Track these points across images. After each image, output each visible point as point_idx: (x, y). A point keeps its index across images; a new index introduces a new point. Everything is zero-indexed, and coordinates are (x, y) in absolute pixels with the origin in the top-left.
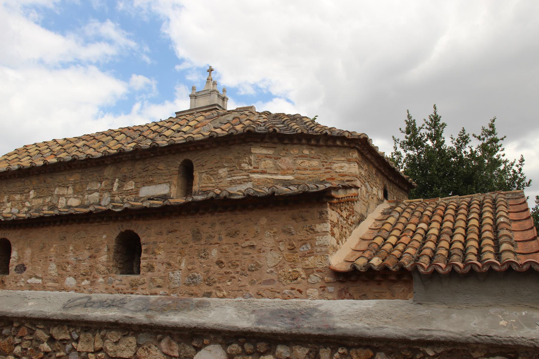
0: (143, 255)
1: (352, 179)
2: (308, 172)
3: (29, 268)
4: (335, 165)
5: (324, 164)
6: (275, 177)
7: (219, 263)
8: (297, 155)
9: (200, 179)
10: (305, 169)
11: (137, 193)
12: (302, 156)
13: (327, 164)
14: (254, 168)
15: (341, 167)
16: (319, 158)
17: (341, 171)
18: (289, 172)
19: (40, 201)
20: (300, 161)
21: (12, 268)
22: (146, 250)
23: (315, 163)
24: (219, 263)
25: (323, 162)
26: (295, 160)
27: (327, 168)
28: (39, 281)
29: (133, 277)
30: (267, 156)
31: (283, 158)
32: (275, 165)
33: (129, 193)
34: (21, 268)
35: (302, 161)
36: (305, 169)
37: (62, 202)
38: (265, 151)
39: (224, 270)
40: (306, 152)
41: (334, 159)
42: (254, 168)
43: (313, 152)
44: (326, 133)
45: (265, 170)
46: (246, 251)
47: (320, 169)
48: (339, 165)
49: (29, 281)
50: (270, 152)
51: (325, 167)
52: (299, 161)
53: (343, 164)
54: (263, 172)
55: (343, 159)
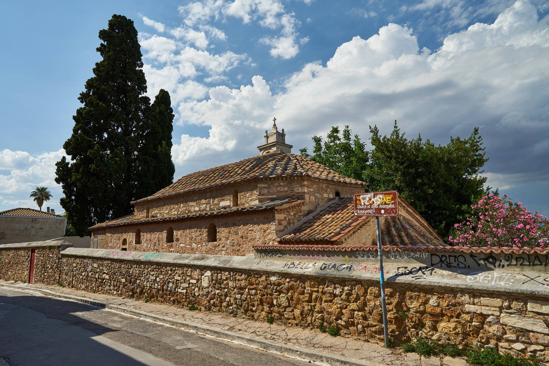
0: (218, 234)
3: (180, 240)
6: (268, 197)
7: (242, 237)
9: (240, 198)
10: (282, 192)
11: (219, 204)
19: (184, 208)
20: (279, 188)
21: (174, 240)
22: (219, 232)
24: (242, 237)
28: (184, 245)
29: (215, 243)
33: (216, 204)
34: (178, 240)
37: (193, 208)
38: (263, 185)
39: (244, 240)
40: (282, 184)
46: (250, 232)
49: (181, 245)
50: (266, 185)
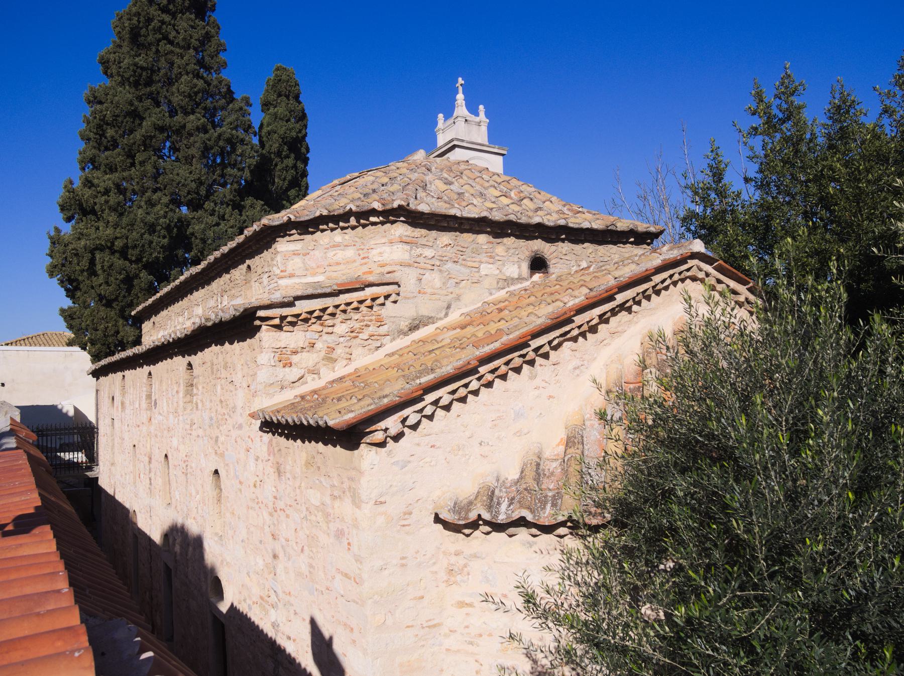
1: (394, 269)
2: (342, 267)
4: (374, 252)
5: (361, 252)
8: (328, 246)
10: (338, 264)
12: (334, 246)
13: (364, 251)
14: (282, 271)
15: (381, 253)
16: (354, 245)
17: (380, 259)
18: (318, 270)
20: (332, 254)
23: (350, 253)
25: (358, 250)
26: (325, 253)
27: (364, 258)
30: (295, 253)
31: (312, 253)
32: (303, 263)
35: (334, 252)
36: (338, 264)
41: (373, 242)
42: (282, 271)
43: (347, 237)
44: (351, 209)
45: (293, 272)
47: (355, 261)
48: (378, 250)
51: (362, 256)
52: (331, 254)
53: (384, 248)
54: (291, 276)
55: (383, 241)
